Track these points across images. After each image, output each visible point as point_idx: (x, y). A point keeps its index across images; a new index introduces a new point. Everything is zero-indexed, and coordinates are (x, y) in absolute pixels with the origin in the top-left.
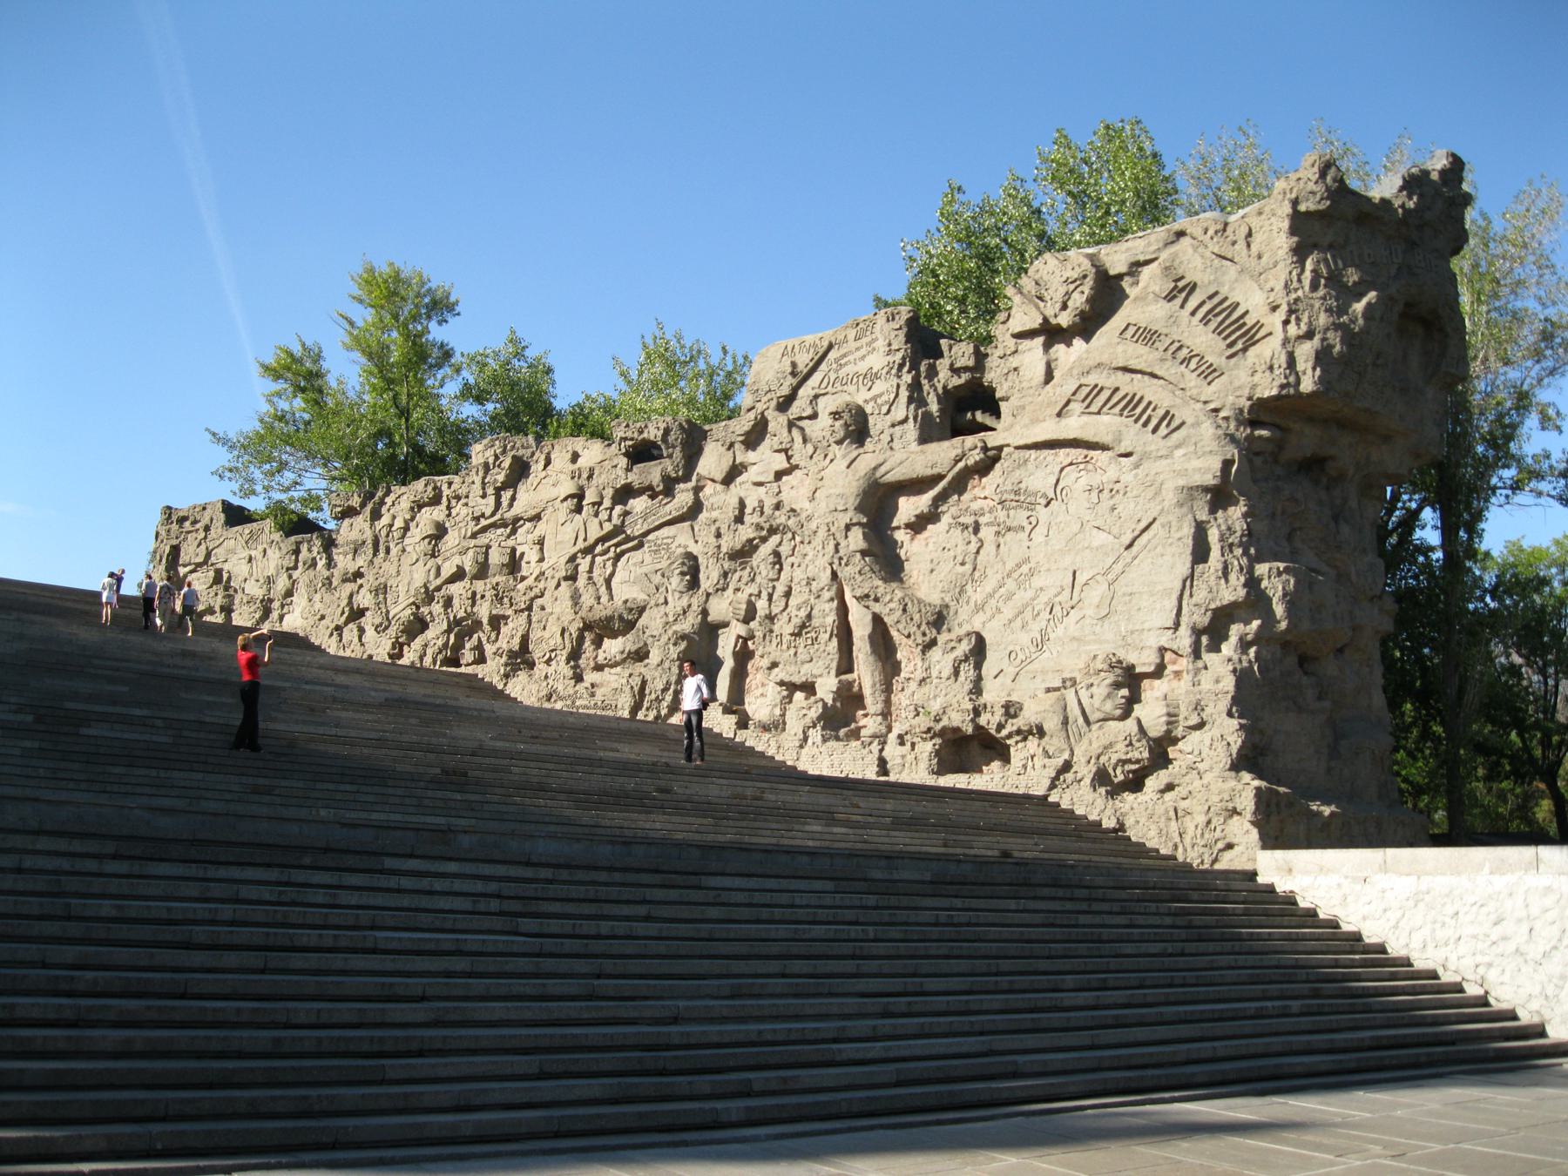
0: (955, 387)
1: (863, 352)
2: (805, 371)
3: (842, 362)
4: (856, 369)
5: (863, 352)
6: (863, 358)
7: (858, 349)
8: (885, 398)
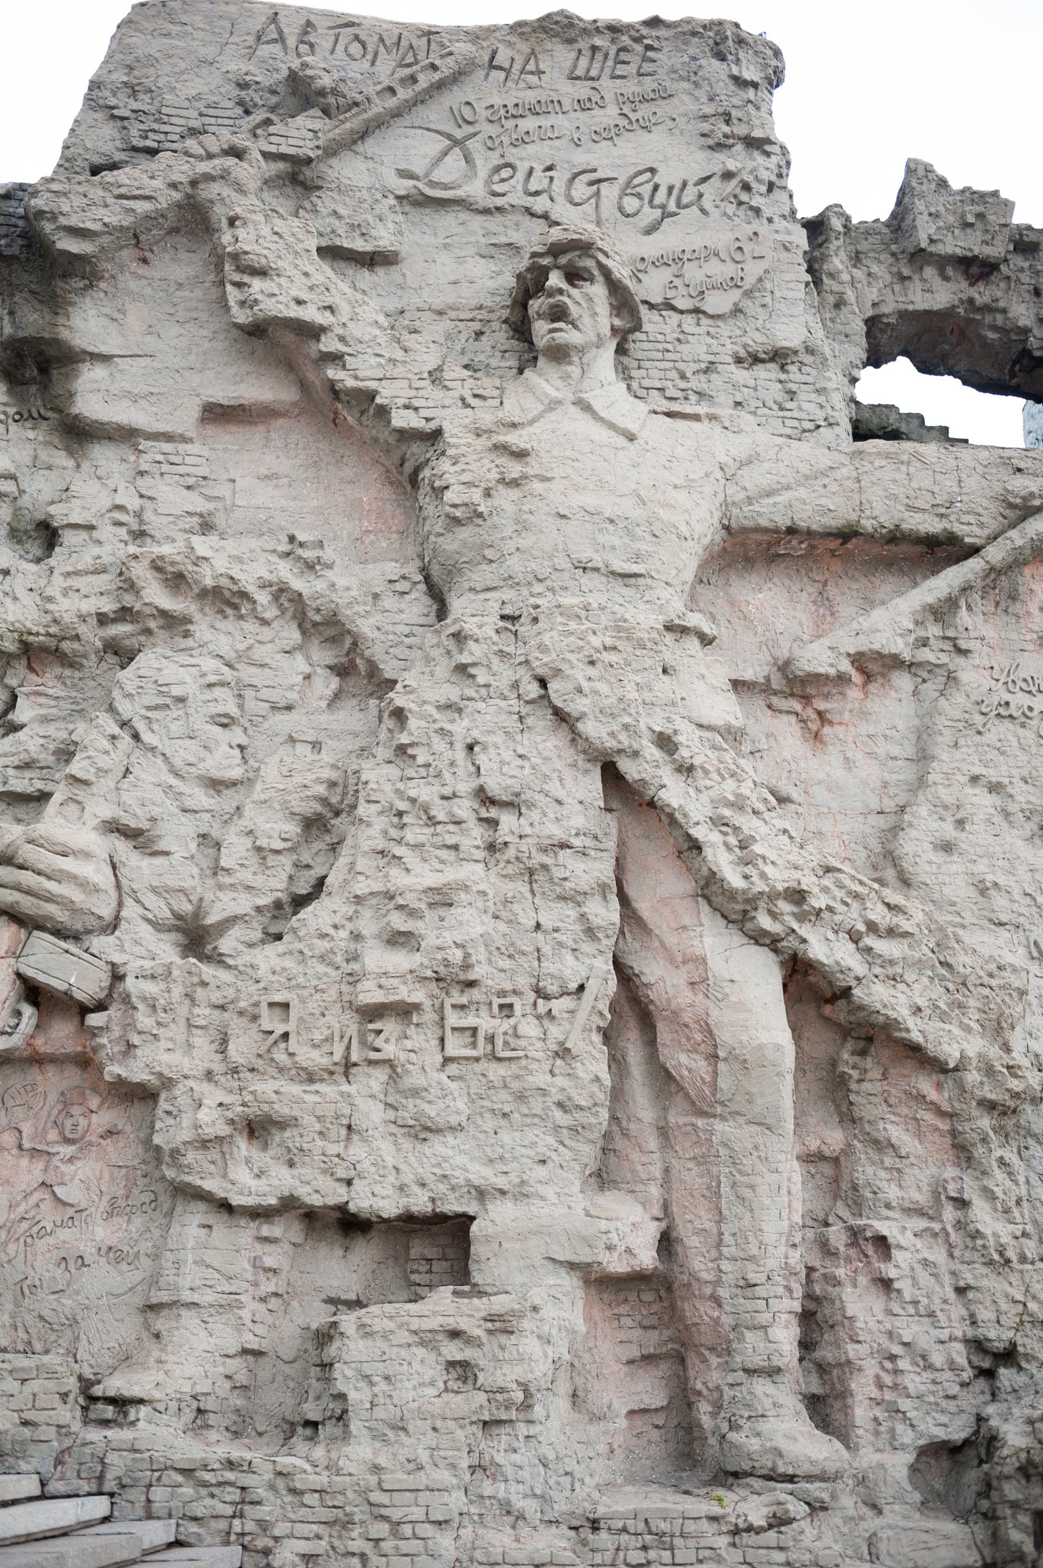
0: (903, 315)
1: (608, 116)
2: (379, 106)
3: (529, 123)
4: (581, 158)
5: (608, 116)
6: (607, 135)
7: (583, 106)
8: (719, 270)
